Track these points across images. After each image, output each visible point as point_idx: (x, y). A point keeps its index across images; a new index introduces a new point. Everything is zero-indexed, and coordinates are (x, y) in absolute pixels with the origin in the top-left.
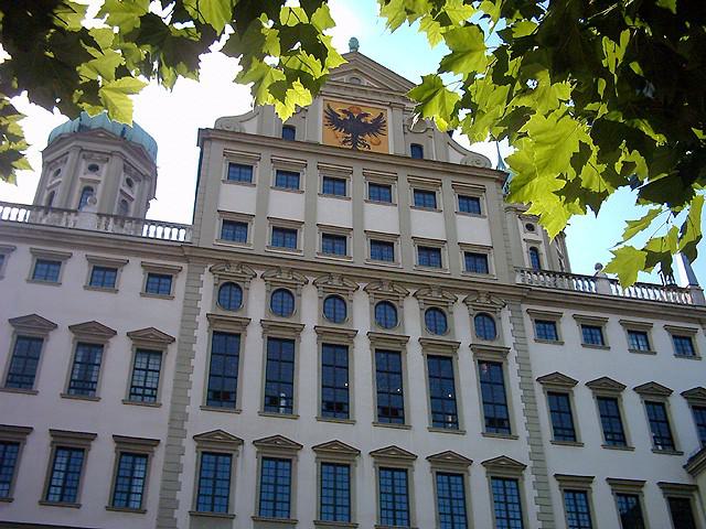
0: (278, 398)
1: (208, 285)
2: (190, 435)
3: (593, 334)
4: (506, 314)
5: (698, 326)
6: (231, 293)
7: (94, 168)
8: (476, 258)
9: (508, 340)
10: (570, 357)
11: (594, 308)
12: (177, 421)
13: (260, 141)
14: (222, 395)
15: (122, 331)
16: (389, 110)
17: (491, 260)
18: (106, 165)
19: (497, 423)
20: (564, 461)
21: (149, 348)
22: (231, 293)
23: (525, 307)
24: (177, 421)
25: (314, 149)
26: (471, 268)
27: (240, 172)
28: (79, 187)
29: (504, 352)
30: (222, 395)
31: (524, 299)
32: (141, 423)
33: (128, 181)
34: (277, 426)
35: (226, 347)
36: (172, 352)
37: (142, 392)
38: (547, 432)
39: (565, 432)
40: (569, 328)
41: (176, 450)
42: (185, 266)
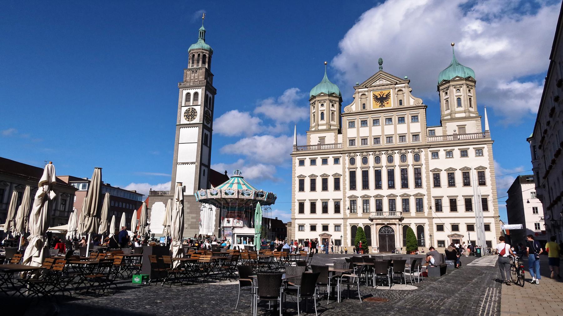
0: (366, 186)
1: (347, 159)
6: (352, 161)
14: (353, 186)
17: (420, 136)
19: (418, 185)
20: (437, 192)
22: (352, 161)
30: (353, 186)
31: (429, 148)
32: (338, 195)
33: (333, 105)
34: (366, 192)
35: (353, 175)
37: (337, 187)
39: (437, 184)
40: (442, 153)
41: (345, 201)
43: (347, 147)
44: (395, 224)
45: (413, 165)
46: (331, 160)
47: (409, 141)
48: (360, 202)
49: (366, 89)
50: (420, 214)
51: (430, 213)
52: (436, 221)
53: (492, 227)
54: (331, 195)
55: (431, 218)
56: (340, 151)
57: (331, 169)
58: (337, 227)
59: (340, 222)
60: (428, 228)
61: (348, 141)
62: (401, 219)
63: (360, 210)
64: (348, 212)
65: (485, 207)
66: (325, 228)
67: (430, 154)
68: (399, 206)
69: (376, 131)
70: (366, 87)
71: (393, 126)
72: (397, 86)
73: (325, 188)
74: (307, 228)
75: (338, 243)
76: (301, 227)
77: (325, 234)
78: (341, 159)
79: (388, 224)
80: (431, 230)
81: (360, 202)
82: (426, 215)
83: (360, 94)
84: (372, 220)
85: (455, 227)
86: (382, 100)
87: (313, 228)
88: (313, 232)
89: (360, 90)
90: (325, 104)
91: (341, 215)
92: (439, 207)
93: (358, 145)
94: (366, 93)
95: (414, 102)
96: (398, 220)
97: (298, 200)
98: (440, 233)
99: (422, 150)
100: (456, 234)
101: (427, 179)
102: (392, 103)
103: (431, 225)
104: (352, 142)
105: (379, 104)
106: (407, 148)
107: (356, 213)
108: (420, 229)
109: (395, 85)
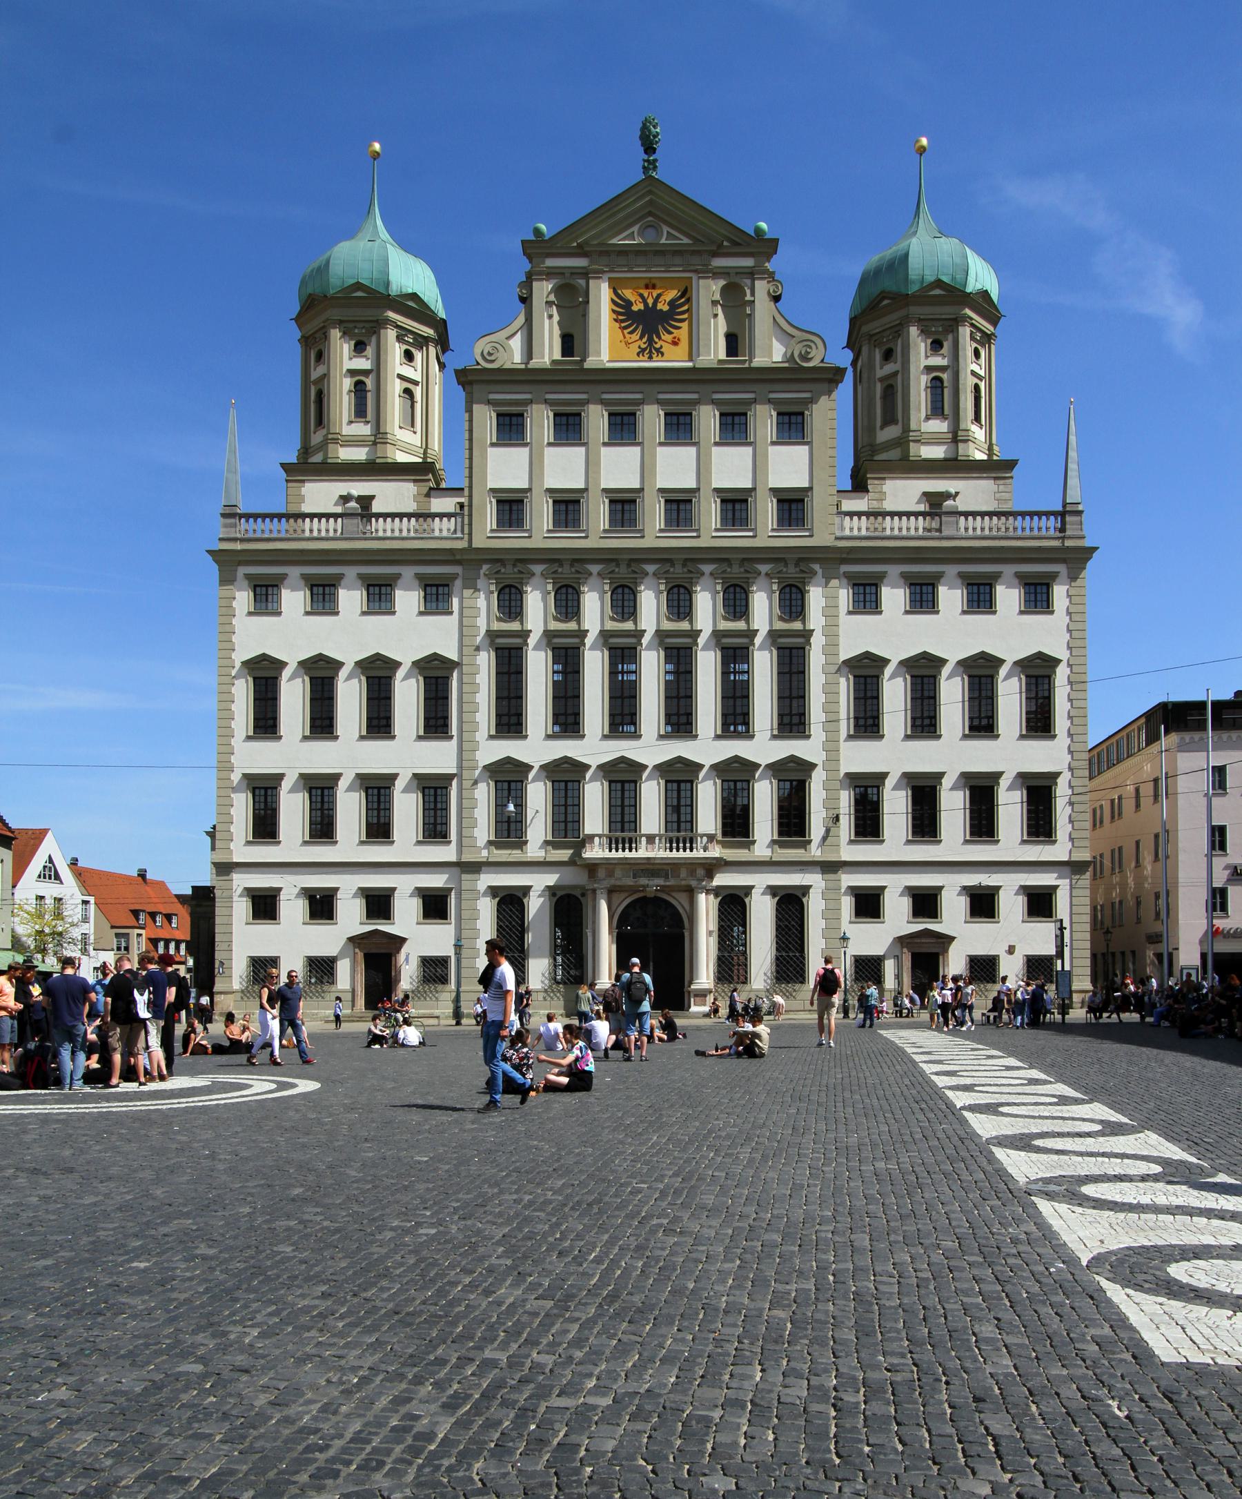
2: (481, 764)
3: (923, 598)
5: (1061, 568)
8: (792, 505)
9: (815, 618)
10: (894, 631)
13: (530, 379)
14: (510, 721)
19: (792, 721)
20: (861, 757)
23: (845, 568)
27: (511, 428)
29: (807, 634)
30: (510, 721)
32: (439, 757)
37: (436, 723)
38: (844, 728)
39: (867, 723)
42: (457, 569)
45: (773, 635)
48: (538, 796)
49: (581, 262)
54: (408, 754)
56: (451, 551)
57: (410, 631)
58: (434, 906)
60: (822, 905)
63: (538, 829)
64: (483, 830)
65: (1040, 824)
66: (379, 904)
68: (708, 817)
70: (581, 252)
72: (719, 262)
74: (292, 908)
75: (434, 970)
80: (831, 915)
81: (538, 796)
82: (815, 852)
84: (592, 868)
87: (321, 906)
89: (550, 262)
92: (868, 823)
97: (246, 776)
99: (816, 567)
100: (927, 933)
101: (827, 695)
103: (830, 895)
104: (511, 507)
106: (750, 559)
107: (521, 844)
108: (790, 906)
109: (715, 254)
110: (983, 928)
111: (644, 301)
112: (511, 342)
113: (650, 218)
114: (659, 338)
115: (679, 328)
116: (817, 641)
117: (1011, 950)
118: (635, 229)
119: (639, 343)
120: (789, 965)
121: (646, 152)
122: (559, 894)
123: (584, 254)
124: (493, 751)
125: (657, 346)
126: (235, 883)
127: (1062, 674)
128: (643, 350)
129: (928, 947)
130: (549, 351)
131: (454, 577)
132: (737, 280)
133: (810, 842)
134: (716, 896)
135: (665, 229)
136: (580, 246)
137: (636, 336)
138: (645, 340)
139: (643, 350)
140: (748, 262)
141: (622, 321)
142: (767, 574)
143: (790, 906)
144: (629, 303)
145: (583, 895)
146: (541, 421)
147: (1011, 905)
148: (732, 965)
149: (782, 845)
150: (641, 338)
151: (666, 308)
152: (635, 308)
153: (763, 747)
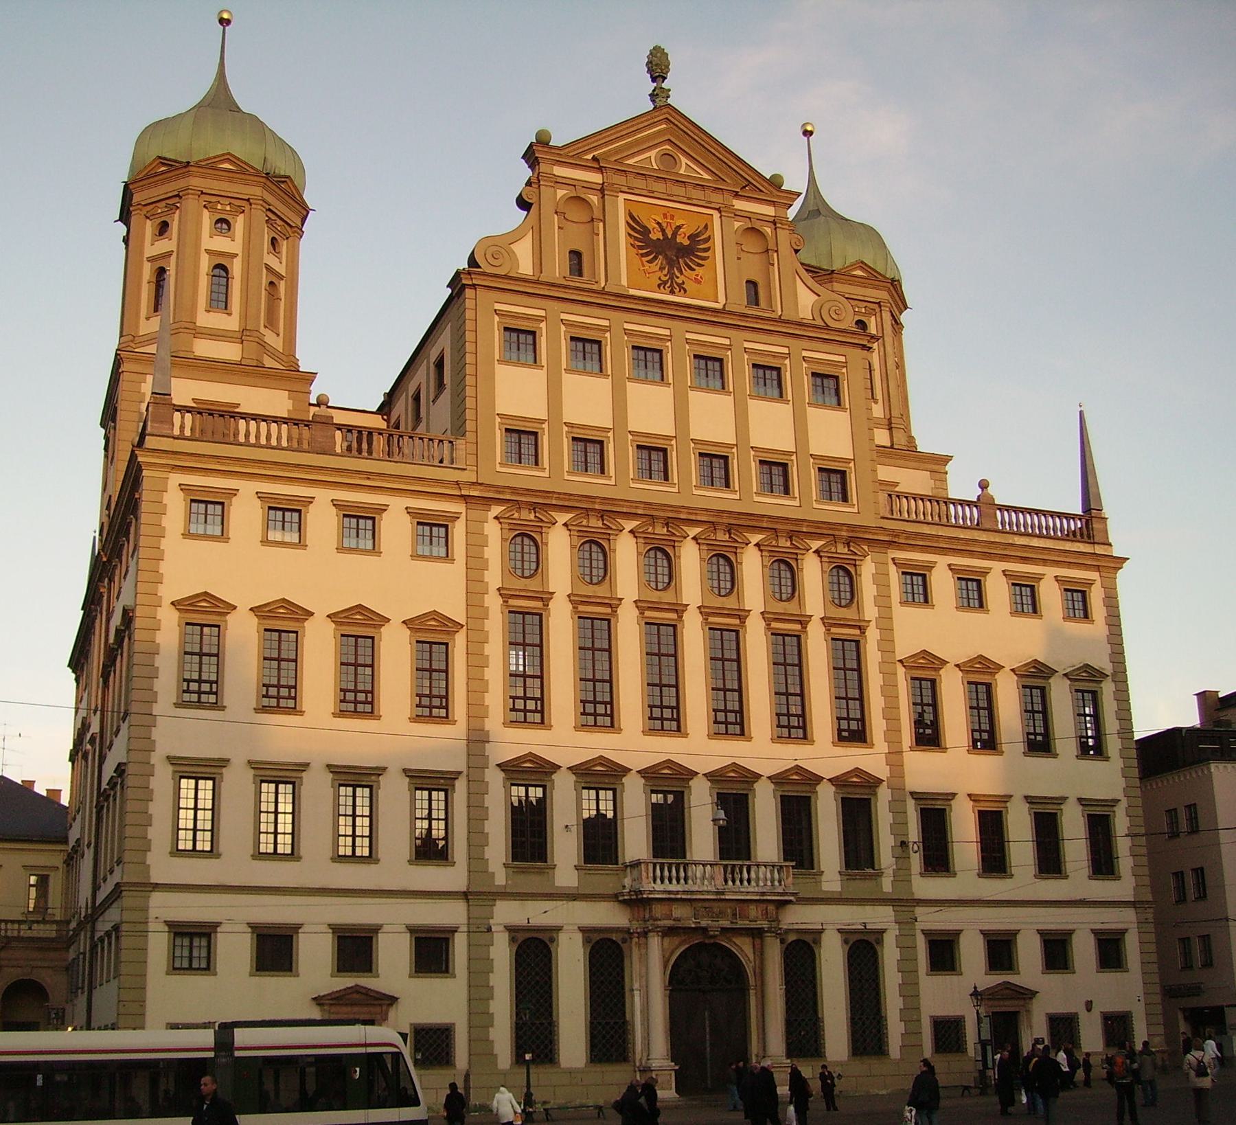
1: (493, 531)
4: (867, 570)
5: (1094, 575)
7: (223, 224)
8: (835, 478)
9: (870, 612)
11: (971, 554)
12: (477, 740)
15: (396, 617)
16: (716, 214)
18: (240, 219)
21: (433, 637)
24: (477, 740)
25: (621, 303)
26: (828, 495)
28: (205, 264)
31: (891, 544)
33: (274, 241)
36: (459, 644)
37: (432, 704)
38: (907, 737)
39: (929, 735)
43: (498, 466)
44: (756, 934)
46: (396, 526)
47: (806, 501)
49: (596, 178)
50: (861, 888)
51: (902, 876)
52: (931, 920)
53: (1132, 947)
55: (904, 904)
57: (404, 582)
58: (431, 952)
59: (450, 914)
61: (498, 435)
62: (782, 904)
66: (355, 948)
67: (894, 574)
68: (767, 839)
69: (651, 408)
70: (597, 165)
71: (727, 401)
72: (739, 205)
73: (358, 699)
74: (234, 949)
76: (194, 944)
77: (357, 989)
78: (459, 531)
79: (724, 930)
83: (561, 193)
84: (636, 902)
85: (1000, 950)
86: (675, 252)
87: (275, 949)
88: (274, 984)
89: (559, 171)
90: (239, 223)
91: (452, 877)
93: (556, 470)
94: (594, 199)
95: (818, 309)
96: (771, 908)
98: (943, 981)
100: (1007, 985)
102: (718, 281)
104: (523, 437)
105: (656, 270)
108: (863, 952)
110: (1056, 979)
111: (663, 231)
112: (515, 248)
113: (667, 147)
114: (681, 273)
115: (700, 265)
116: (873, 635)
117: (1089, 1006)
118: (653, 154)
119: (659, 274)
120: (867, 1032)
121: (654, 79)
122: (596, 937)
123: (601, 170)
124: (512, 742)
125: (679, 281)
126: (153, 913)
127: (1107, 690)
128: (665, 283)
129: (1008, 1006)
130: (557, 269)
131: (455, 517)
132: (757, 225)
133: (880, 875)
134: (782, 941)
135: (684, 160)
136: (595, 159)
137: (655, 266)
138: (665, 272)
139: (665, 283)
140: (769, 211)
141: (640, 248)
142: (817, 552)
143: (863, 952)
144: (646, 231)
145: (624, 941)
146: (554, 343)
147: (1084, 950)
148: (804, 1033)
149: (851, 878)
150: (661, 269)
151: (686, 242)
152: (653, 236)
153: (825, 756)
